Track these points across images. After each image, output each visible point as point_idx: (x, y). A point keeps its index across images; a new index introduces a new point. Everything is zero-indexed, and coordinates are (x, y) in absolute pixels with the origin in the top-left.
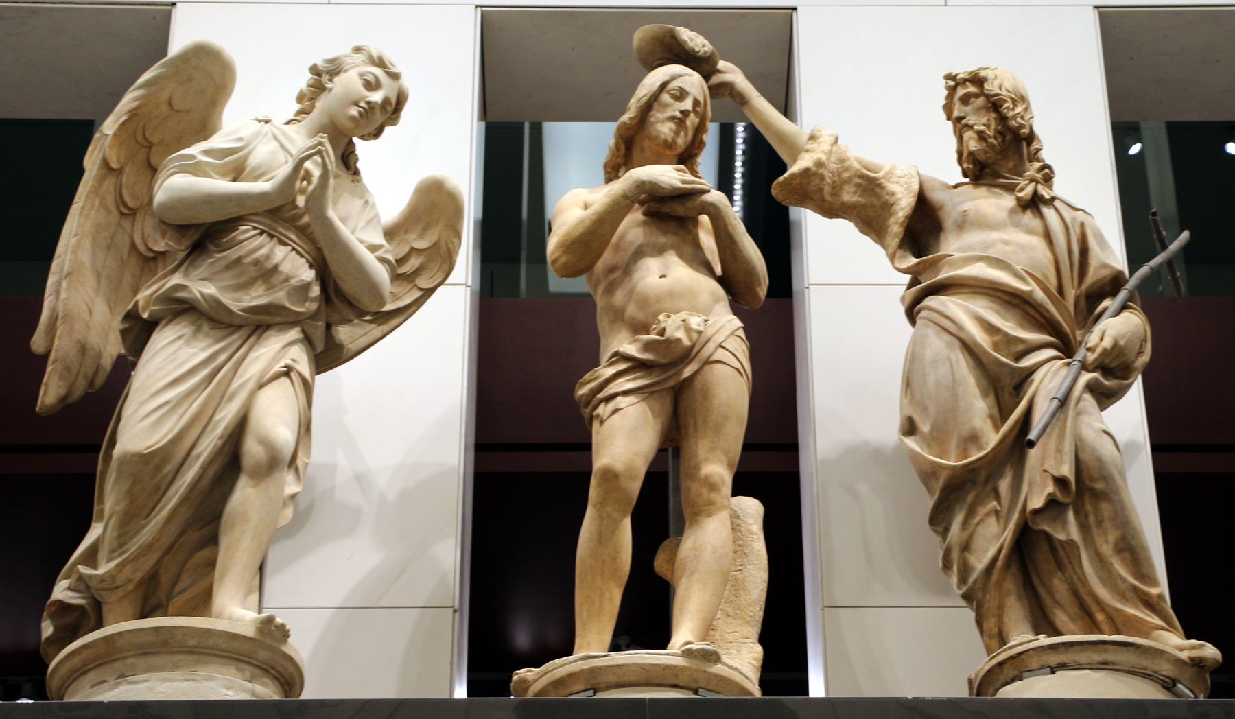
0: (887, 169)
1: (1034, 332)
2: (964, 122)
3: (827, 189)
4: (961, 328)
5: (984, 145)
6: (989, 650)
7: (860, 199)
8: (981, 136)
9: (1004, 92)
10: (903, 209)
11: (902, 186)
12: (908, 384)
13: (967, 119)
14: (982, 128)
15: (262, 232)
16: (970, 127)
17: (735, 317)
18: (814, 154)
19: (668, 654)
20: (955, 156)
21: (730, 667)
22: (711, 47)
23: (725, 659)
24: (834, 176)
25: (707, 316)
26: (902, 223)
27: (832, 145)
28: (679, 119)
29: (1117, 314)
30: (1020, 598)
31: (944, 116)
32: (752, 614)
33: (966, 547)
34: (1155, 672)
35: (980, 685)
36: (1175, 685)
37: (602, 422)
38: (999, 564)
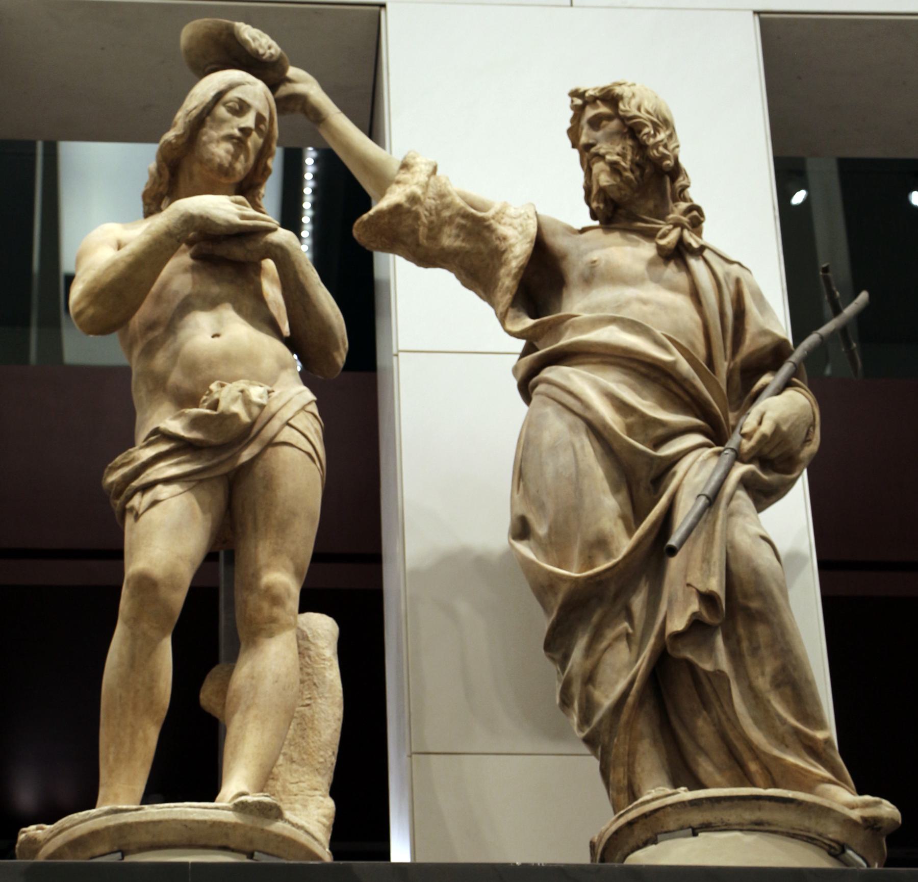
0: (497, 207)
1: (676, 412)
2: (593, 150)
3: (422, 231)
4: (587, 406)
5: (618, 179)
6: (616, 808)
7: (464, 245)
8: (615, 168)
9: (643, 114)
10: (516, 257)
11: (515, 228)
12: (520, 475)
13: (598, 146)
14: (615, 158)
16: (602, 157)
17: (304, 388)
18: (407, 186)
19: (217, 808)
20: (582, 193)
21: (293, 825)
22: (279, 49)
23: (288, 815)
24: (431, 214)
25: (271, 386)
26: (516, 275)
27: (429, 177)
28: (238, 138)
29: (779, 391)
30: (655, 742)
31: (568, 143)
32: (321, 760)
33: (590, 679)
34: (820, 835)
35: (604, 849)
36: (843, 851)
37: (137, 517)
38: (630, 700)
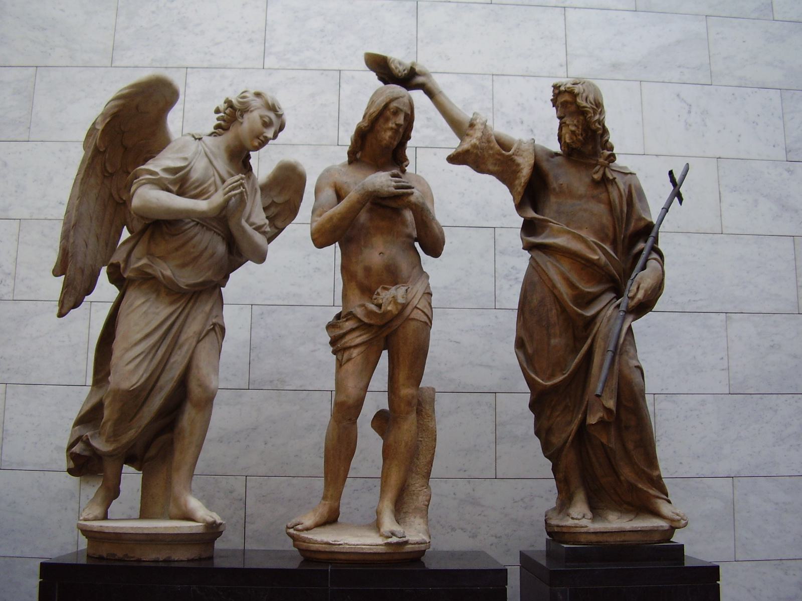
15: (198, 223)
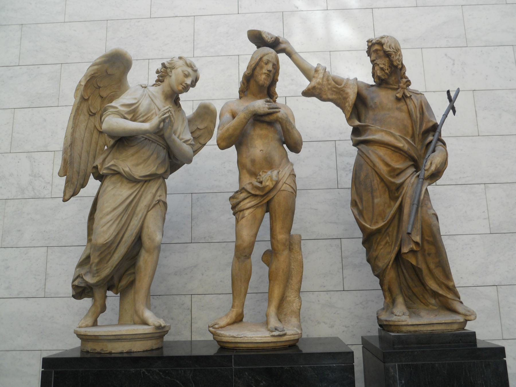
2: (375, 62)
5: (384, 73)
16: (378, 65)
20: (371, 75)
